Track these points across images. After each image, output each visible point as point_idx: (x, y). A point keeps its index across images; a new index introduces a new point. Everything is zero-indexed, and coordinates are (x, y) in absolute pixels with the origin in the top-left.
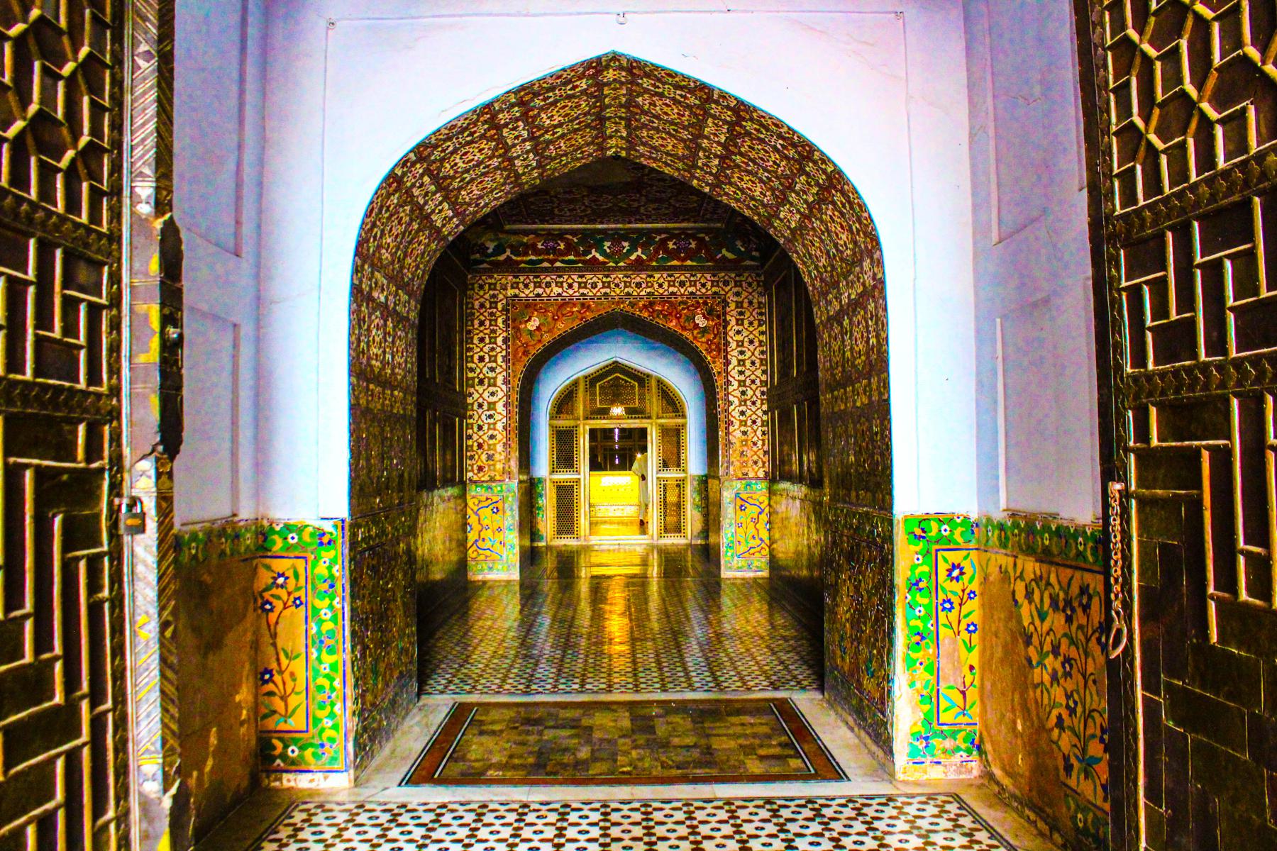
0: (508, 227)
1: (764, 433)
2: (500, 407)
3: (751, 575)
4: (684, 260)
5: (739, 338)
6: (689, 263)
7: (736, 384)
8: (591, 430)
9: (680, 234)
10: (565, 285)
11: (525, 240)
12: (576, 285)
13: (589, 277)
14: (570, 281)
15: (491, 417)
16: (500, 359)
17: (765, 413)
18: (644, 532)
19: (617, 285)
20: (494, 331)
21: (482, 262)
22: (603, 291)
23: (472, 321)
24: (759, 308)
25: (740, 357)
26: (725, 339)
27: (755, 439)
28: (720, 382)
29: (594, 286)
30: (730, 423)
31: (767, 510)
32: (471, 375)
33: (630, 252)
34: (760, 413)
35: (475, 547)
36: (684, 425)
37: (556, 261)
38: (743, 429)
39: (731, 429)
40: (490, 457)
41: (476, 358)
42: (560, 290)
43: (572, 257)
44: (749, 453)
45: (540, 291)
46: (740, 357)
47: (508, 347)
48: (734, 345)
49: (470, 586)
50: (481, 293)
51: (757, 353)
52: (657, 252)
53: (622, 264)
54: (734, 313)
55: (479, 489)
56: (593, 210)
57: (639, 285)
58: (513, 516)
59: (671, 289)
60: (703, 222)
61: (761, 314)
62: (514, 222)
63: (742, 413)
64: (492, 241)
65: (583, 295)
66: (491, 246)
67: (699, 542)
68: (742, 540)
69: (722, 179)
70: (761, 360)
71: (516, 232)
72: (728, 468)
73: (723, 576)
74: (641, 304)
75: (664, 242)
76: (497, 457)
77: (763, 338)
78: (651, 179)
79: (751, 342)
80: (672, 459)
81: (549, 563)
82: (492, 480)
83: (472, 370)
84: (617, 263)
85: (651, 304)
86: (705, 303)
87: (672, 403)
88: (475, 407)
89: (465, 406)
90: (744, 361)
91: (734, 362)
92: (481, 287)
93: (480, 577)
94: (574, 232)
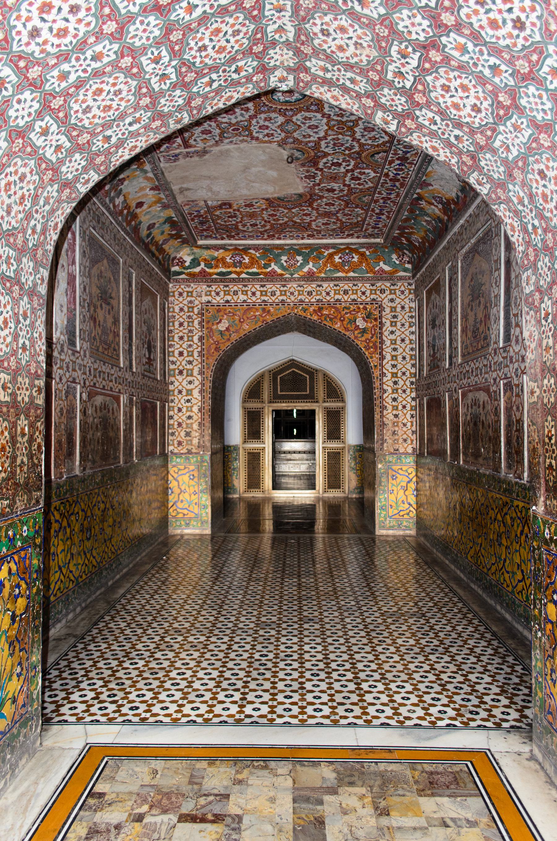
0: (200, 242)
1: (412, 416)
2: (196, 393)
3: (401, 533)
5: (392, 337)
6: (352, 274)
7: (389, 375)
9: (345, 249)
10: (249, 293)
11: (216, 254)
12: (258, 294)
13: (270, 287)
15: (188, 401)
17: (413, 399)
18: (312, 486)
19: (292, 294)
21: (179, 273)
22: (281, 298)
24: (410, 312)
25: (393, 353)
26: (381, 338)
27: (405, 421)
28: (376, 373)
30: (384, 408)
31: (414, 479)
32: (172, 367)
33: (302, 266)
35: (174, 507)
36: (343, 408)
38: (394, 412)
39: (385, 412)
41: (176, 353)
42: (245, 298)
43: (255, 270)
44: (400, 433)
45: (229, 298)
46: (393, 353)
47: (203, 344)
48: (388, 343)
49: (171, 540)
50: (181, 299)
51: (407, 350)
52: (325, 265)
53: (296, 276)
54: (389, 316)
55: (178, 460)
56: (272, 225)
57: (310, 293)
58: (206, 482)
59: (337, 297)
60: (365, 237)
61: (412, 317)
62: (206, 237)
63: (395, 400)
64: (189, 255)
65: (264, 301)
66: (188, 260)
67: (354, 496)
68: (394, 504)
69: (418, 97)
70: (411, 356)
71: (207, 247)
72: (382, 444)
73: (377, 533)
74: (311, 309)
75: (331, 256)
76: (194, 434)
77: (413, 337)
78: (321, 190)
79: (403, 340)
80: (334, 431)
81: (241, 514)
82: (189, 452)
83: (173, 363)
84: (292, 275)
85: (320, 309)
86: (365, 308)
87: (334, 391)
88: (176, 392)
89: (167, 392)
90: (396, 356)
91: (388, 357)
93: (179, 532)
94: (256, 248)
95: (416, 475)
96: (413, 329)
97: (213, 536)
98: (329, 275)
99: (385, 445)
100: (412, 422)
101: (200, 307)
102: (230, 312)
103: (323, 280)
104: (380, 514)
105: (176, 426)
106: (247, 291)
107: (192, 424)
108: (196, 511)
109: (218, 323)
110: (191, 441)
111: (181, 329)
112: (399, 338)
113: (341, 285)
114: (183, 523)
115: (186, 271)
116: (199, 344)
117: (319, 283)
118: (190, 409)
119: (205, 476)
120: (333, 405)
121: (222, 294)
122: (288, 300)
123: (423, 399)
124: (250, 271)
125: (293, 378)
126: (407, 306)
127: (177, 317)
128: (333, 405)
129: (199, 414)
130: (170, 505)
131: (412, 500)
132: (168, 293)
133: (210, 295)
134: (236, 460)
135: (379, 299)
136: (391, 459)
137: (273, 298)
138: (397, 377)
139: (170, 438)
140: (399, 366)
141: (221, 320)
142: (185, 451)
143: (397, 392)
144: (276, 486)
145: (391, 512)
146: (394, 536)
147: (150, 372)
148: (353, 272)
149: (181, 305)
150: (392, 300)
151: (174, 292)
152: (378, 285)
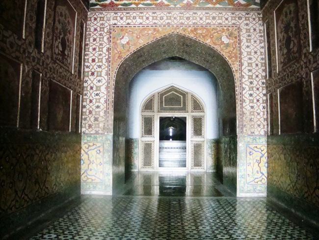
1: (264, 108)
2: (103, 89)
3: (256, 195)
4: (215, 4)
5: (248, 50)
7: (247, 77)
8: (160, 117)
10: (144, 18)
12: (151, 18)
13: (159, 14)
14: (147, 16)
15: (97, 95)
16: (104, 61)
17: (264, 95)
20: (101, 44)
22: (167, 21)
23: (89, 38)
24: (260, 33)
25: (249, 61)
26: (240, 50)
27: (259, 111)
28: (237, 76)
29: (162, 18)
30: (243, 101)
31: (266, 155)
34: (261, 95)
35: (85, 174)
37: (139, 4)
38: (251, 105)
40: (96, 119)
41: (90, 60)
42: (141, 21)
44: (255, 120)
45: (129, 21)
46: (249, 61)
50: (95, 22)
51: (259, 59)
53: (178, 6)
54: (245, 35)
55: (89, 139)
57: (188, 18)
59: (208, 21)
61: (261, 36)
63: (251, 95)
65: (155, 23)
67: (210, 171)
70: (262, 63)
72: (242, 128)
74: (189, 29)
76: (100, 119)
77: (263, 50)
79: (256, 53)
80: (198, 131)
82: (97, 133)
83: (88, 67)
84: (175, 5)
85: (196, 30)
87: (197, 106)
88: (89, 87)
90: (251, 64)
92: (95, 19)
93: (88, 193)
95: (268, 152)
96: (262, 45)
97: (113, 197)
98: (202, 6)
99: (244, 129)
100: (263, 112)
101: (108, 27)
102: (130, 31)
103: (199, 9)
104: (240, 181)
105: (87, 113)
106: (142, 17)
107: (99, 111)
108: (101, 178)
109: (121, 39)
110: (99, 124)
111: (95, 43)
112: (253, 51)
113: (210, 13)
114: (91, 186)
115: (100, 3)
116: (107, 53)
117: (195, 11)
118: (98, 101)
119: (108, 151)
120: (197, 114)
121: (124, 18)
122: (173, 23)
123: (275, 91)
124: (145, 2)
125: (173, 98)
126: (257, 29)
127: (92, 34)
128: (197, 114)
129: (105, 105)
130: (82, 173)
131: (265, 170)
132: (86, 16)
133: (116, 19)
134: (136, 148)
135: (238, 23)
136: (249, 139)
137: (162, 21)
138: (252, 79)
139: (83, 122)
140: (254, 71)
141: (123, 37)
142: (93, 132)
143: (253, 90)
144: (160, 165)
145: (249, 179)
146: (251, 198)
147: (63, 63)
148: (219, 4)
149: (95, 27)
150: (247, 25)
151: (91, 18)
152: (237, 13)
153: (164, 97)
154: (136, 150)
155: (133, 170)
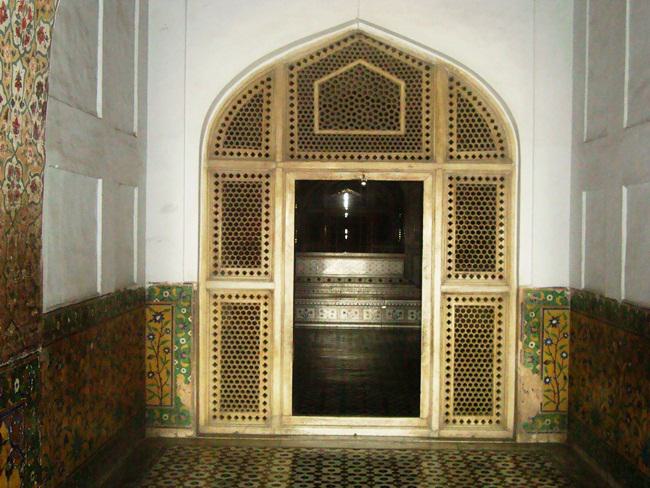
80: (477, 247)
87: (478, 129)
134: (185, 327)
153: (316, 84)
154: (183, 341)
155: (170, 434)
